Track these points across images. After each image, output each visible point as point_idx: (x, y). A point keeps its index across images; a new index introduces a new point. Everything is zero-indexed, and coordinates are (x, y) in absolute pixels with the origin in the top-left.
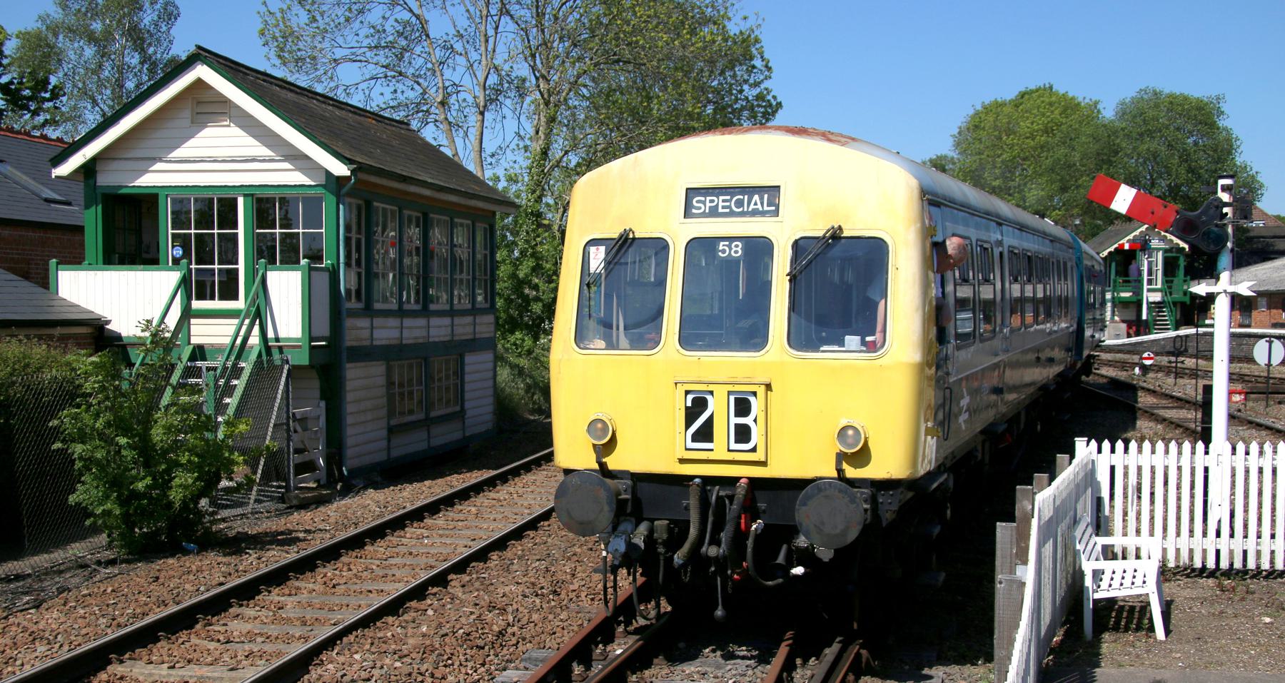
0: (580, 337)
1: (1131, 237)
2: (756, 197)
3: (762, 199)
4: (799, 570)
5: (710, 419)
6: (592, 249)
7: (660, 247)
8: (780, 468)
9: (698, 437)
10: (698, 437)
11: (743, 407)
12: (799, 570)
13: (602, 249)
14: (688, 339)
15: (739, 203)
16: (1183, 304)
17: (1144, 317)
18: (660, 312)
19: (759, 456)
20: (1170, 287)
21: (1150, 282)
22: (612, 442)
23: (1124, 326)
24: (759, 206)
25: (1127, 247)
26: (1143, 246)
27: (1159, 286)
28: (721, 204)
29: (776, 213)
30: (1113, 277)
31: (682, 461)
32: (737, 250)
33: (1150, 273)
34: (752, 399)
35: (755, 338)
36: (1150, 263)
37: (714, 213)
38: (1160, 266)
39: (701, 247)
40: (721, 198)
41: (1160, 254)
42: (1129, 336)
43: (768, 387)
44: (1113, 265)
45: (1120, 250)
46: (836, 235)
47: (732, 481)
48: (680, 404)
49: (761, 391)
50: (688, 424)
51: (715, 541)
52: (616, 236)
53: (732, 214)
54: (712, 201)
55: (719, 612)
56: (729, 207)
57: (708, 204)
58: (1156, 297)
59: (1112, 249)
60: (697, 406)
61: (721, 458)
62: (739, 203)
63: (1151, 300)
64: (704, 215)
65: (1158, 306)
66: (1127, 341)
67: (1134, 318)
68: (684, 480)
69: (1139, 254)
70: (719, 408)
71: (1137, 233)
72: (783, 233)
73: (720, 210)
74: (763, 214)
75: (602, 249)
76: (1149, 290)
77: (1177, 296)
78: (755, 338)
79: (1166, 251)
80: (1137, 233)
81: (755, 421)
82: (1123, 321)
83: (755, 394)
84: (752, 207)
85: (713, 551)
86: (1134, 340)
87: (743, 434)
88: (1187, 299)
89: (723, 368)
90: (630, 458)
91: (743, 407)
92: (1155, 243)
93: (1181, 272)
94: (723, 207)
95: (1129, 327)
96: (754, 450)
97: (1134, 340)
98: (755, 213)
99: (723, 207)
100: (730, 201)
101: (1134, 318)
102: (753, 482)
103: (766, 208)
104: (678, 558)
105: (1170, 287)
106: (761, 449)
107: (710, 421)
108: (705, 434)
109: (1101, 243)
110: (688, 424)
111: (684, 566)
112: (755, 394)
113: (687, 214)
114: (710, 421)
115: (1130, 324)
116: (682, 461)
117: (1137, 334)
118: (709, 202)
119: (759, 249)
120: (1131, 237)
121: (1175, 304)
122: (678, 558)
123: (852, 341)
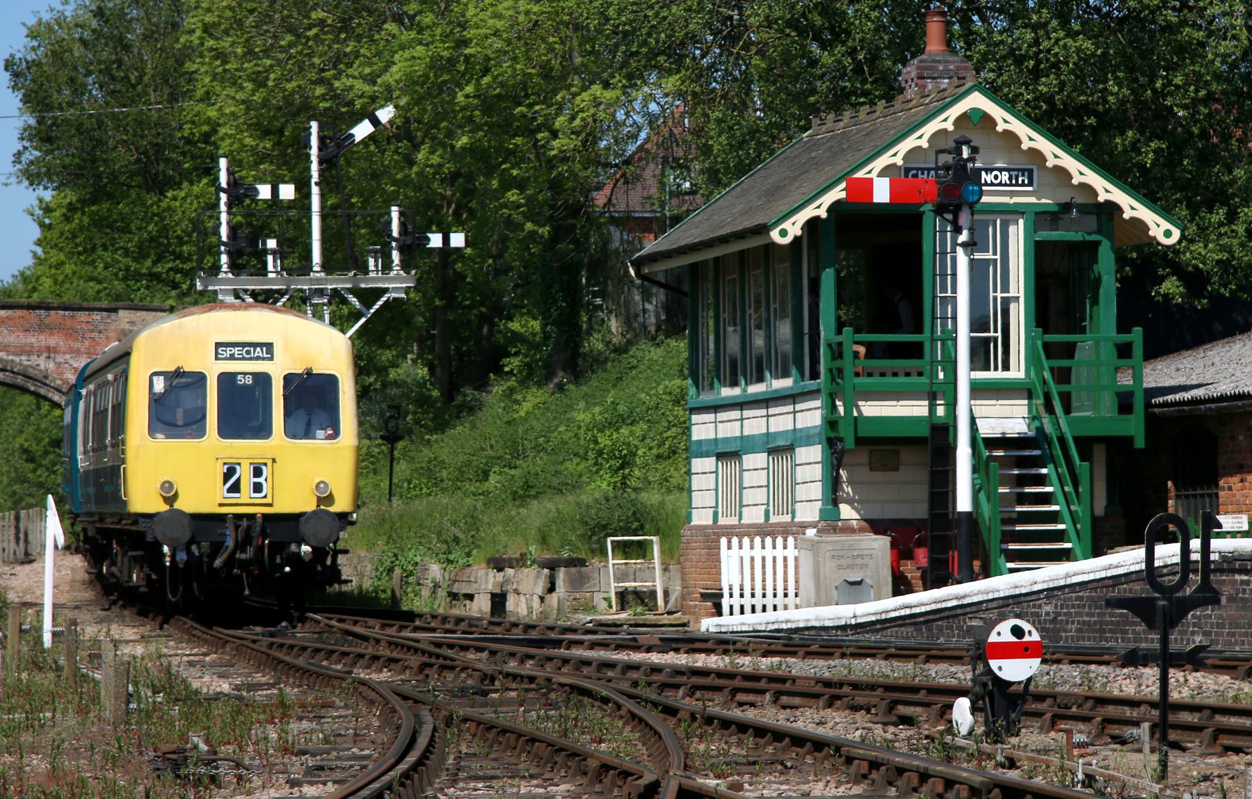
0: (152, 431)
1: (896, 156)
4: (287, 569)
5: (239, 479)
6: (155, 378)
7: (200, 378)
8: (283, 506)
9: (229, 491)
10: (229, 491)
11: (258, 472)
12: (287, 569)
13: (162, 378)
14: (227, 430)
15: (248, 352)
16: (1117, 446)
17: (964, 503)
18: (204, 417)
19: (268, 501)
20: (1063, 376)
21: (981, 354)
22: (176, 496)
23: (880, 545)
25: (882, 193)
26: (953, 185)
27: (1017, 372)
29: (271, 359)
30: (826, 331)
31: (221, 505)
32: (249, 380)
33: (979, 323)
34: (264, 468)
35: (263, 431)
36: (978, 270)
37: (232, 357)
38: (1019, 285)
39: (226, 380)
41: (1018, 235)
42: (901, 586)
43: (274, 461)
44: (828, 279)
45: (853, 219)
46: (309, 373)
47: (251, 517)
48: (221, 470)
49: (269, 463)
50: (225, 482)
51: (243, 551)
52: (172, 369)
53: (244, 359)
55: (247, 592)
58: (1009, 419)
59: (820, 209)
60: (230, 473)
61: (246, 502)
62: (248, 352)
63: (988, 429)
64: (226, 359)
65: (1010, 458)
66: (891, 605)
67: (918, 509)
68: (221, 518)
69: (932, 224)
70: (245, 475)
71: (921, 139)
72: (277, 370)
74: (263, 359)
75: (162, 378)
76: (978, 390)
77: (1095, 414)
78: (263, 431)
79: (1041, 218)
80: (921, 139)
82: (876, 526)
83: (265, 464)
85: (243, 556)
86: (923, 599)
87: (258, 488)
88: (1134, 427)
89: (245, 449)
90: (190, 503)
91: (258, 472)
92: (997, 189)
93: (1106, 311)
95: (901, 552)
97: (923, 599)
98: (258, 358)
101: (918, 509)
102: (265, 516)
104: (218, 563)
105: (1063, 376)
106: (269, 496)
107: (238, 480)
108: (235, 488)
109: (774, 193)
110: (225, 482)
111: (221, 568)
112: (265, 464)
113: (217, 358)
114: (238, 480)
115: (904, 538)
116: (221, 505)
117: (936, 578)
118: (229, 351)
119: (263, 380)
120: (896, 156)
121: (1086, 445)
122: (218, 563)
123: (320, 433)
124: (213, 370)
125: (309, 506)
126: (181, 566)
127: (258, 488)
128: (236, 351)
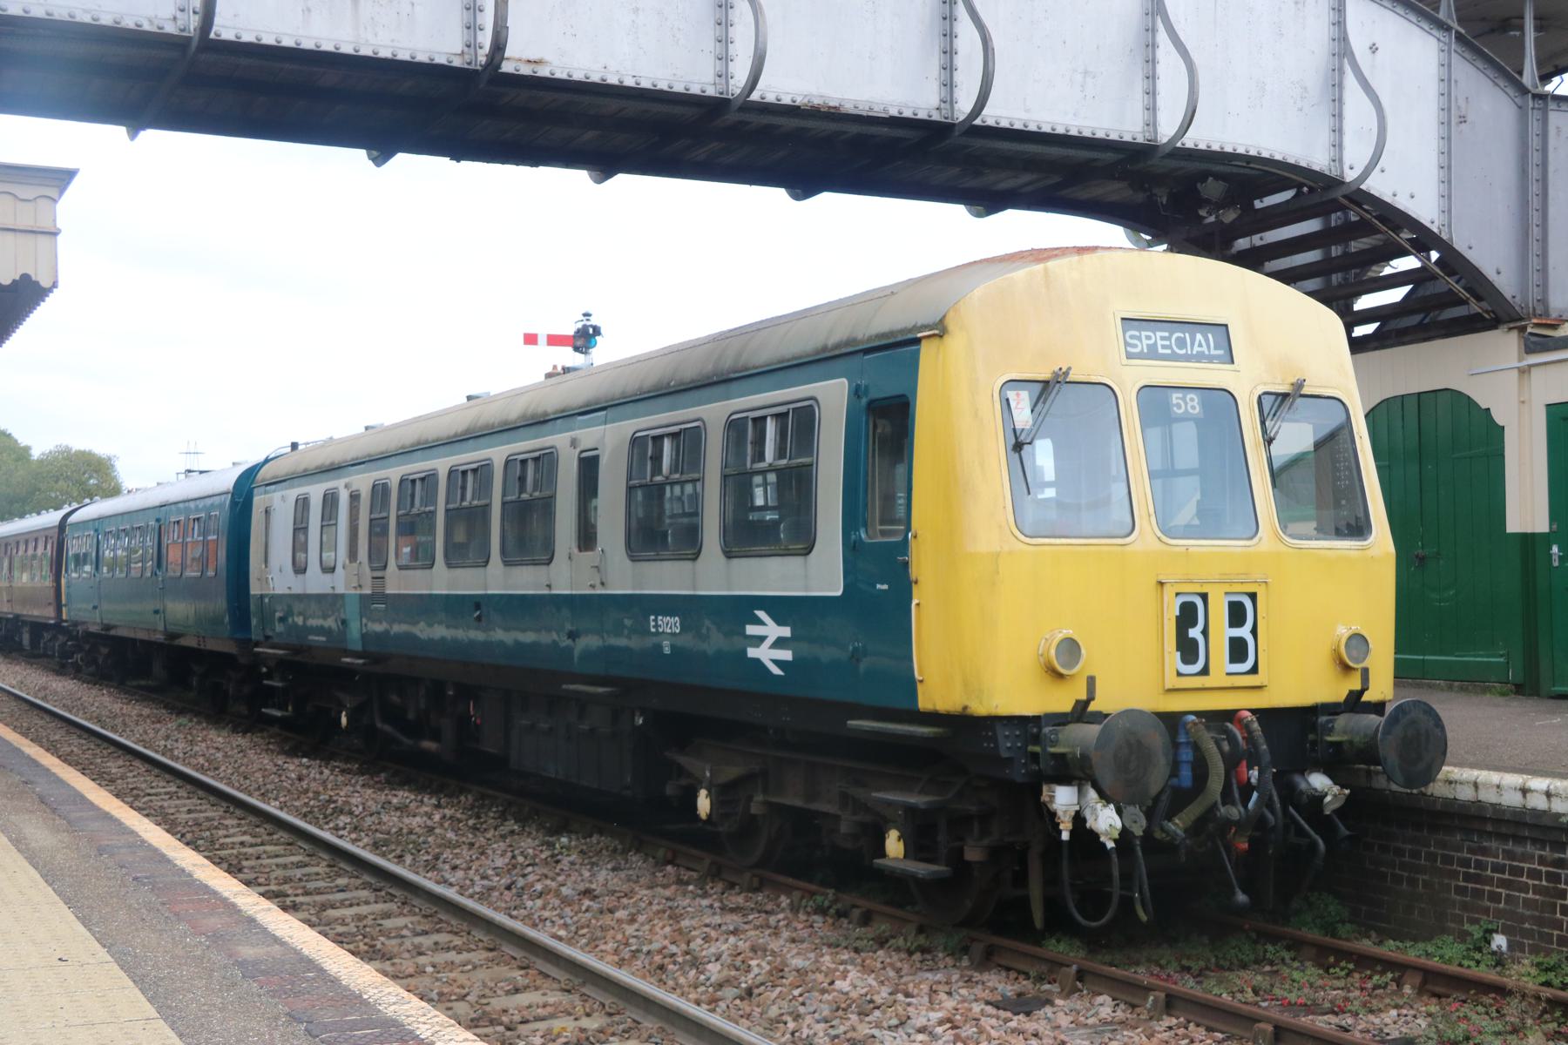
2: (1199, 337)
3: (1207, 340)
13: (1025, 395)
15: (1181, 343)
24: (1205, 348)
28: (1160, 343)
37: (1152, 354)
39: (1154, 397)
40: (1159, 334)
47: (1230, 715)
53: (1174, 357)
54: (1148, 338)
56: (1169, 347)
57: (1145, 342)
60: (1187, 615)
64: (1140, 356)
72: (1247, 380)
73: (1161, 351)
74: (1210, 359)
75: (1025, 395)
81: (1254, 632)
84: (1196, 349)
91: (1237, 614)
94: (1164, 347)
96: (1254, 670)
98: (1199, 358)
99: (1164, 347)
100: (1169, 339)
103: (1213, 352)
113: (1129, 356)
118: (1147, 338)
124: (1130, 378)
125: (1333, 690)
126: (1110, 845)
127: (1238, 650)
128: (1158, 337)
